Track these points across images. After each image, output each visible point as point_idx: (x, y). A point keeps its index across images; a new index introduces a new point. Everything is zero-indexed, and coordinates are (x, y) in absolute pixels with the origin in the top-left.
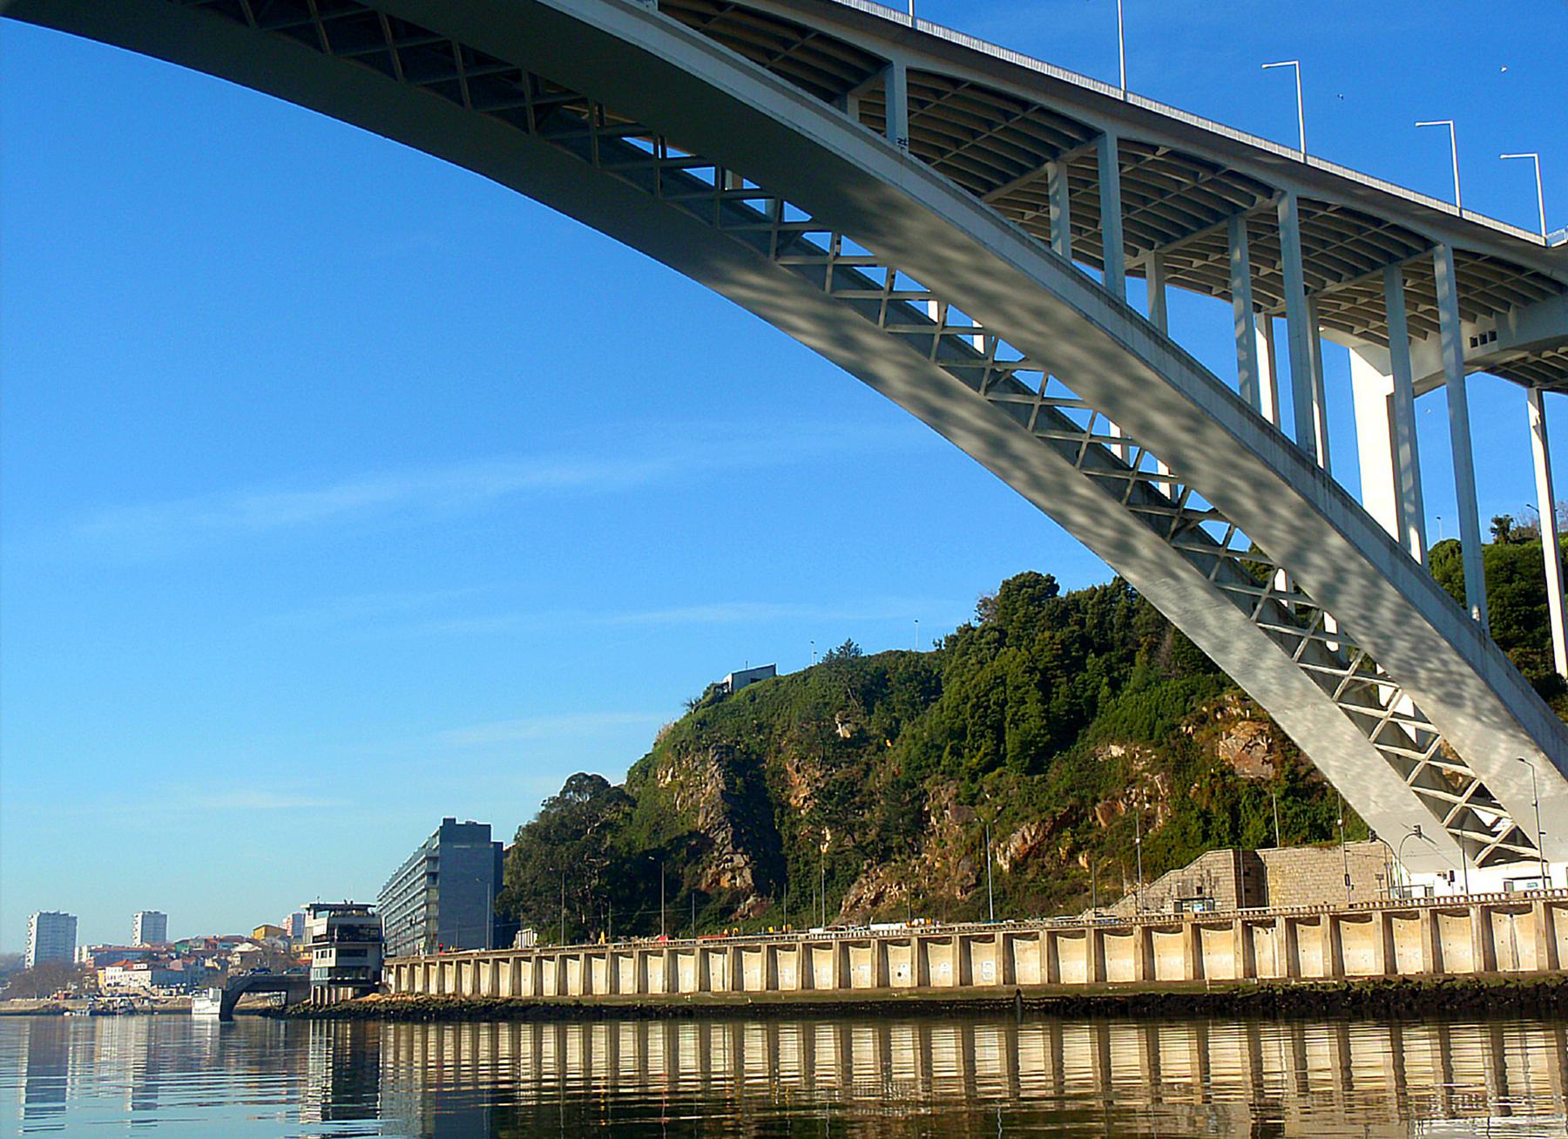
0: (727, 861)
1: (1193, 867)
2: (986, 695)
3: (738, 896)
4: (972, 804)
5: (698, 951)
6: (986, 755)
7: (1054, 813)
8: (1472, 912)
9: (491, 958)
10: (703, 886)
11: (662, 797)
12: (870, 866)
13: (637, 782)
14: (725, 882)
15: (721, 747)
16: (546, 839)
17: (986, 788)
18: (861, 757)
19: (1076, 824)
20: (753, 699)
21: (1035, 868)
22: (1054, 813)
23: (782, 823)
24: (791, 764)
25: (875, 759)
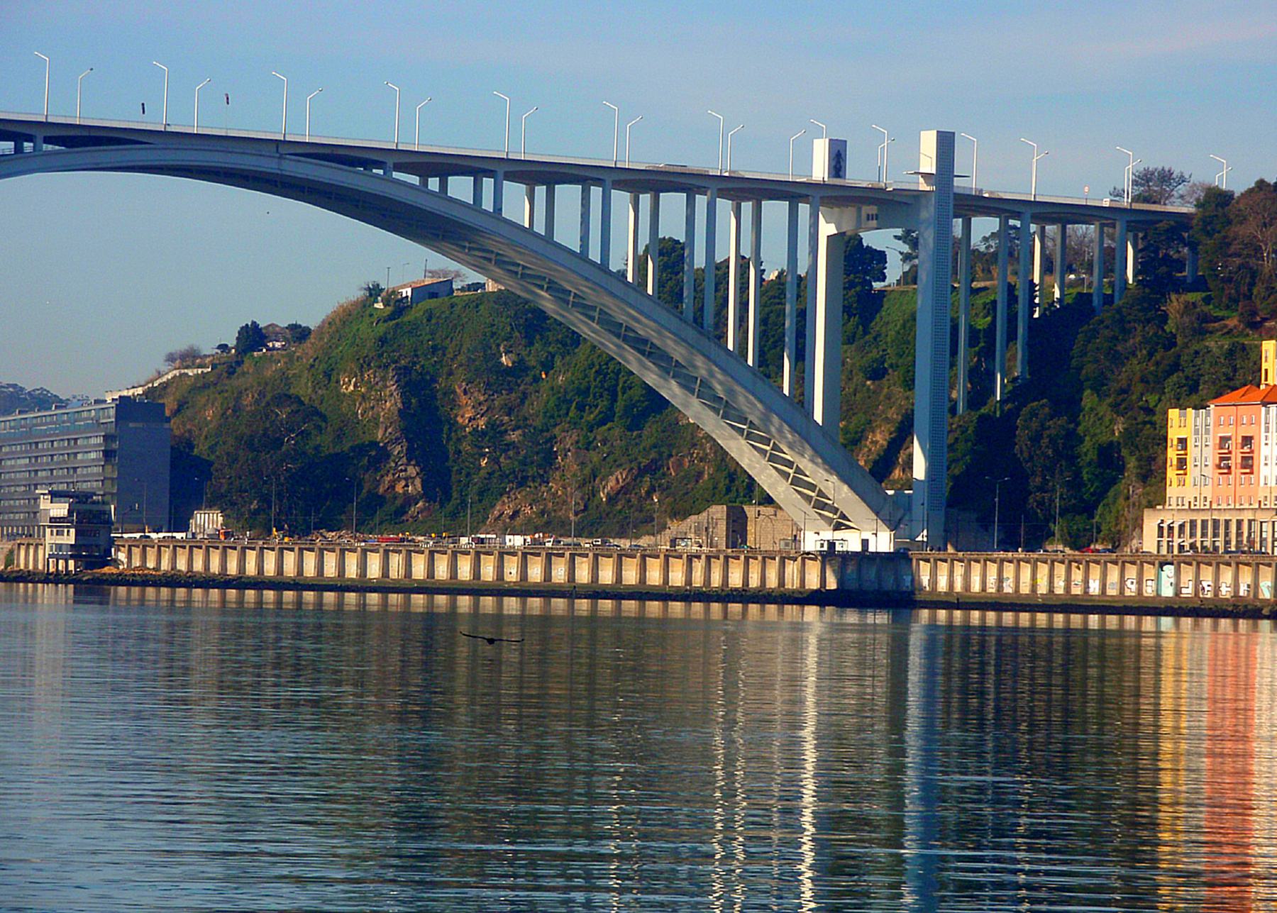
0: (402, 471)
1: (705, 514)
2: (607, 364)
3: (409, 500)
4: (587, 449)
5: (381, 550)
6: (600, 412)
7: (640, 463)
8: (777, 559)
9: (221, 546)
10: (381, 490)
11: (345, 404)
12: (511, 489)
13: (322, 385)
14: (399, 488)
15: (400, 368)
16: (250, 445)
17: (599, 437)
18: (519, 386)
19: (653, 472)
20: (429, 320)
21: (623, 501)
22: (640, 463)
23: (449, 439)
24: (460, 387)
25: (531, 389)
